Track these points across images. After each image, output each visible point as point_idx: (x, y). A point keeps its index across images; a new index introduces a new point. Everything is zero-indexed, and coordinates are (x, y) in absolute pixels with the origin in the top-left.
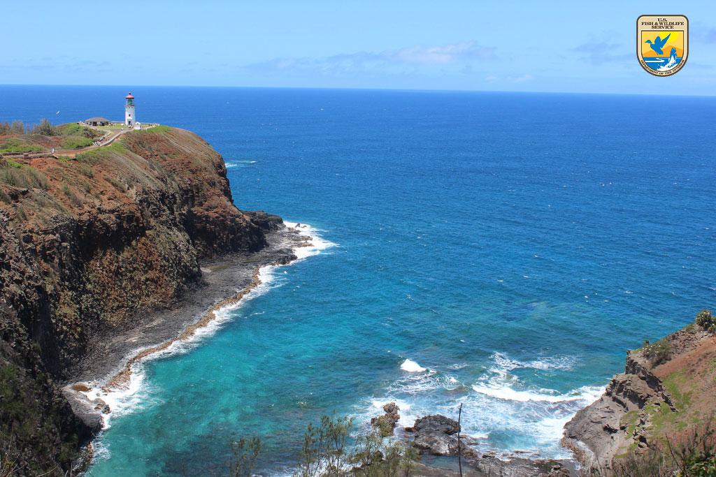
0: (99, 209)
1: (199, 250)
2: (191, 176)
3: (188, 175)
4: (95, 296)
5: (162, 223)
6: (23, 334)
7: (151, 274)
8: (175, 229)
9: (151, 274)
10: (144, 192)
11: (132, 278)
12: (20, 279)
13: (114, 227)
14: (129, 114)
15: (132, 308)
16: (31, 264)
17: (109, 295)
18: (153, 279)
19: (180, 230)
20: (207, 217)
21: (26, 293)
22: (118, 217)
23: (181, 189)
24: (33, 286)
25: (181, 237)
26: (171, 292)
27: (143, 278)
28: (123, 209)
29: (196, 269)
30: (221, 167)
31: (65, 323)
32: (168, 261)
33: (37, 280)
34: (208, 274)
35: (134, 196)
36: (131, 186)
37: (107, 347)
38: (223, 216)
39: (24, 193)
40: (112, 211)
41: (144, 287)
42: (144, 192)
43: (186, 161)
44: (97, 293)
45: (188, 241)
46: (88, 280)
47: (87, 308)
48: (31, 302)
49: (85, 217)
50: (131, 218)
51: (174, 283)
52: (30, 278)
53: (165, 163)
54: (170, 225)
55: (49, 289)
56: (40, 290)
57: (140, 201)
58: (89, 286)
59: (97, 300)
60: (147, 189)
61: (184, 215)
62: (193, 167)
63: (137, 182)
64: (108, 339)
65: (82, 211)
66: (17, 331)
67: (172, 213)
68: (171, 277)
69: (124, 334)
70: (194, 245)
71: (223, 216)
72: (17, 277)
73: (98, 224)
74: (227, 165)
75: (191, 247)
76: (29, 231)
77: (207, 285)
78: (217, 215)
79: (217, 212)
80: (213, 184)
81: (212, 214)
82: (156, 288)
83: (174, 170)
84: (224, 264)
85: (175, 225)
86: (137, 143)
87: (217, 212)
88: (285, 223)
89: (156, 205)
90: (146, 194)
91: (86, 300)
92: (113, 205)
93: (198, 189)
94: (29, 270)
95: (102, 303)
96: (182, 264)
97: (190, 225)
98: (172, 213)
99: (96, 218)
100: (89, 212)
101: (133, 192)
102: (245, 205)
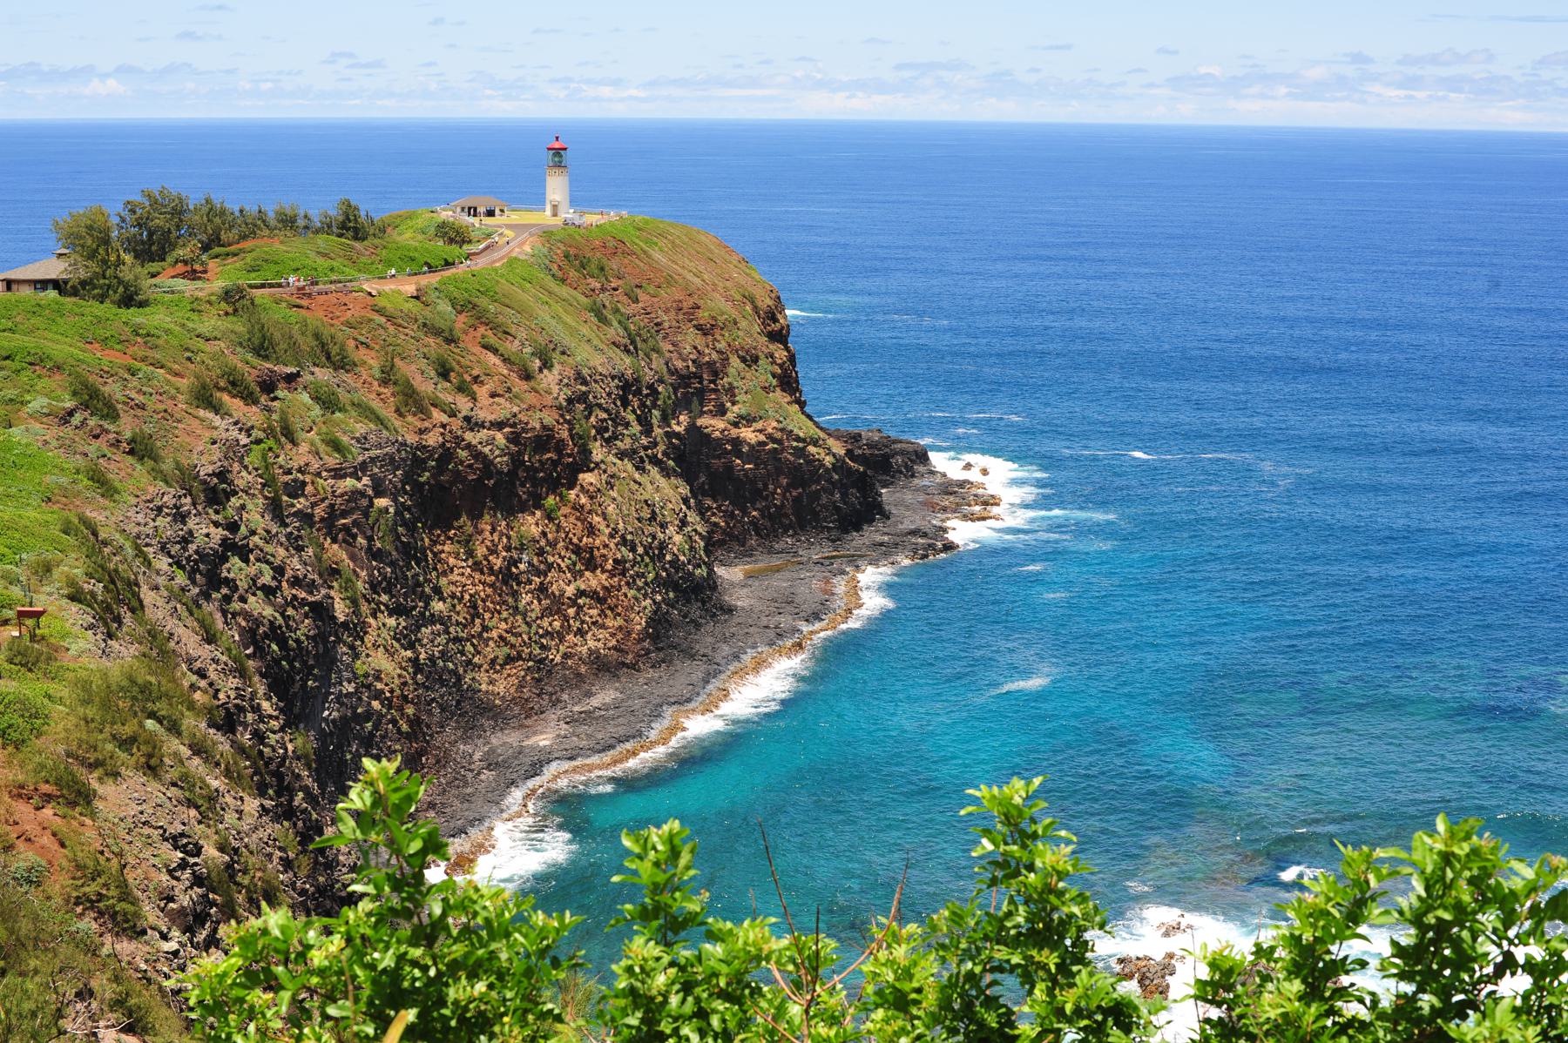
0: (467, 419)
1: (716, 524)
2: (700, 341)
3: (690, 339)
4: (452, 629)
5: (622, 455)
6: (271, 717)
7: (594, 581)
8: (654, 471)
9: (594, 581)
11: (542, 589)
12: (274, 584)
13: (502, 462)
14: (556, 188)
15: (541, 661)
16: (300, 549)
17: (485, 629)
18: (595, 592)
19: (666, 473)
20: (737, 442)
21: (287, 618)
22: (514, 439)
23: (673, 372)
24: (304, 603)
25: (667, 491)
26: (639, 623)
27: (570, 591)
28: (525, 419)
29: (701, 572)
31: (378, 695)
32: (633, 549)
33: (311, 587)
34: (732, 584)
36: (546, 364)
37: (477, 756)
38: (774, 441)
39: (291, 379)
40: (499, 425)
41: (571, 611)
43: (690, 302)
44: (458, 623)
45: (685, 501)
46: (437, 591)
47: (432, 659)
48: (297, 641)
49: (433, 439)
50: (545, 440)
51: (649, 601)
52: (296, 582)
54: (642, 461)
55: (341, 610)
56: (321, 611)
57: (570, 401)
58: (438, 606)
59: (457, 640)
60: (585, 372)
61: (677, 435)
62: (703, 316)
63: (563, 353)
64: (480, 737)
65: (426, 424)
66: (257, 709)
67: (648, 430)
68: (639, 590)
69: (522, 726)
70: (701, 512)
71: (774, 441)
72: (267, 578)
73: (463, 454)
75: (692, 517)
76: (299, 470)
77: (730, 610)
78: (762, 438)
79: (760, 431)
80: (750, 360)
81: (749, 434)
82: (602, 614)
84: (776, 561)
85: (655, 461)
86: (575, 259)
87: (760, 431)
88: (938, 460)
89: (606, 411)
90: (585, 383)
91: (431, 641)
92: (504, 409)
94: (295, 563)
95: (469, 648)
96: (668, 558)
97: (697, 461)
98: (648, 430)
99: (458, 440)
100: (444, 426)
101: (549, 379)
102: (829, 418)
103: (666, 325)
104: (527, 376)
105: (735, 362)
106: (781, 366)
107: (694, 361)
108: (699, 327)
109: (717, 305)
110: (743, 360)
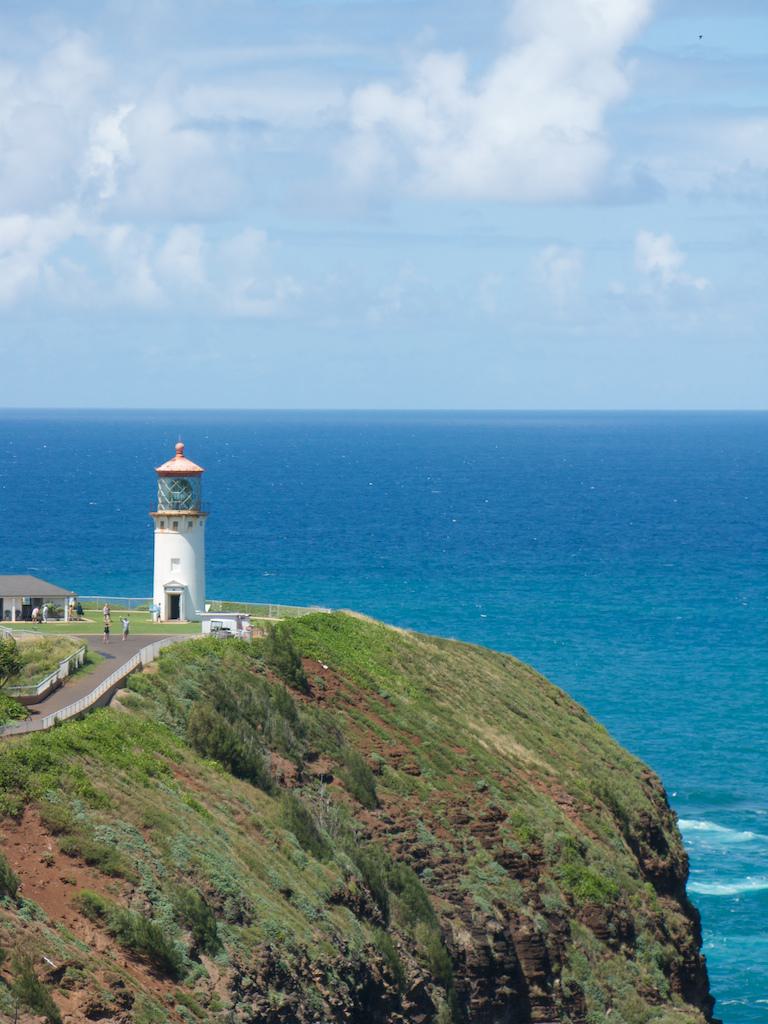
3: (485, 884)
10: (274, 974)
14: (173, 557)
30: (661, 846)
35: (225, 998)
36: (207, 943)
42: (274, 974)
53: (374, 817)
60: (287, 960)
63: (239, 919)
74: (694, 829)
80: (623, 936)
83: (418, 854)
93: (544, 963)
103: (437, 855)
104: (166, 968)
105: (584, 937)
106: (677, 943)
107: (497, 937)
108: (507, 861)
109: (548, 817)
110: (602, 934)
